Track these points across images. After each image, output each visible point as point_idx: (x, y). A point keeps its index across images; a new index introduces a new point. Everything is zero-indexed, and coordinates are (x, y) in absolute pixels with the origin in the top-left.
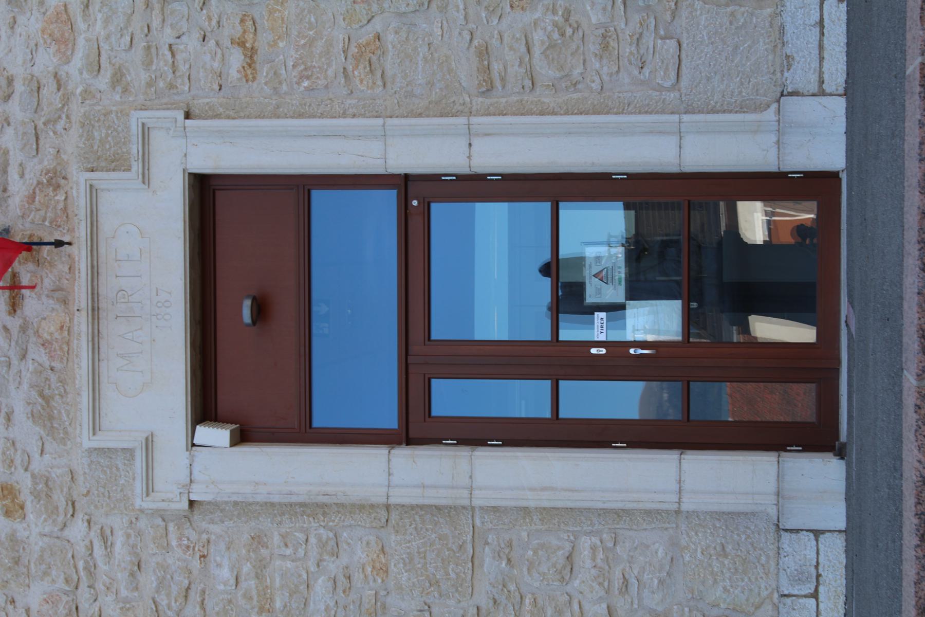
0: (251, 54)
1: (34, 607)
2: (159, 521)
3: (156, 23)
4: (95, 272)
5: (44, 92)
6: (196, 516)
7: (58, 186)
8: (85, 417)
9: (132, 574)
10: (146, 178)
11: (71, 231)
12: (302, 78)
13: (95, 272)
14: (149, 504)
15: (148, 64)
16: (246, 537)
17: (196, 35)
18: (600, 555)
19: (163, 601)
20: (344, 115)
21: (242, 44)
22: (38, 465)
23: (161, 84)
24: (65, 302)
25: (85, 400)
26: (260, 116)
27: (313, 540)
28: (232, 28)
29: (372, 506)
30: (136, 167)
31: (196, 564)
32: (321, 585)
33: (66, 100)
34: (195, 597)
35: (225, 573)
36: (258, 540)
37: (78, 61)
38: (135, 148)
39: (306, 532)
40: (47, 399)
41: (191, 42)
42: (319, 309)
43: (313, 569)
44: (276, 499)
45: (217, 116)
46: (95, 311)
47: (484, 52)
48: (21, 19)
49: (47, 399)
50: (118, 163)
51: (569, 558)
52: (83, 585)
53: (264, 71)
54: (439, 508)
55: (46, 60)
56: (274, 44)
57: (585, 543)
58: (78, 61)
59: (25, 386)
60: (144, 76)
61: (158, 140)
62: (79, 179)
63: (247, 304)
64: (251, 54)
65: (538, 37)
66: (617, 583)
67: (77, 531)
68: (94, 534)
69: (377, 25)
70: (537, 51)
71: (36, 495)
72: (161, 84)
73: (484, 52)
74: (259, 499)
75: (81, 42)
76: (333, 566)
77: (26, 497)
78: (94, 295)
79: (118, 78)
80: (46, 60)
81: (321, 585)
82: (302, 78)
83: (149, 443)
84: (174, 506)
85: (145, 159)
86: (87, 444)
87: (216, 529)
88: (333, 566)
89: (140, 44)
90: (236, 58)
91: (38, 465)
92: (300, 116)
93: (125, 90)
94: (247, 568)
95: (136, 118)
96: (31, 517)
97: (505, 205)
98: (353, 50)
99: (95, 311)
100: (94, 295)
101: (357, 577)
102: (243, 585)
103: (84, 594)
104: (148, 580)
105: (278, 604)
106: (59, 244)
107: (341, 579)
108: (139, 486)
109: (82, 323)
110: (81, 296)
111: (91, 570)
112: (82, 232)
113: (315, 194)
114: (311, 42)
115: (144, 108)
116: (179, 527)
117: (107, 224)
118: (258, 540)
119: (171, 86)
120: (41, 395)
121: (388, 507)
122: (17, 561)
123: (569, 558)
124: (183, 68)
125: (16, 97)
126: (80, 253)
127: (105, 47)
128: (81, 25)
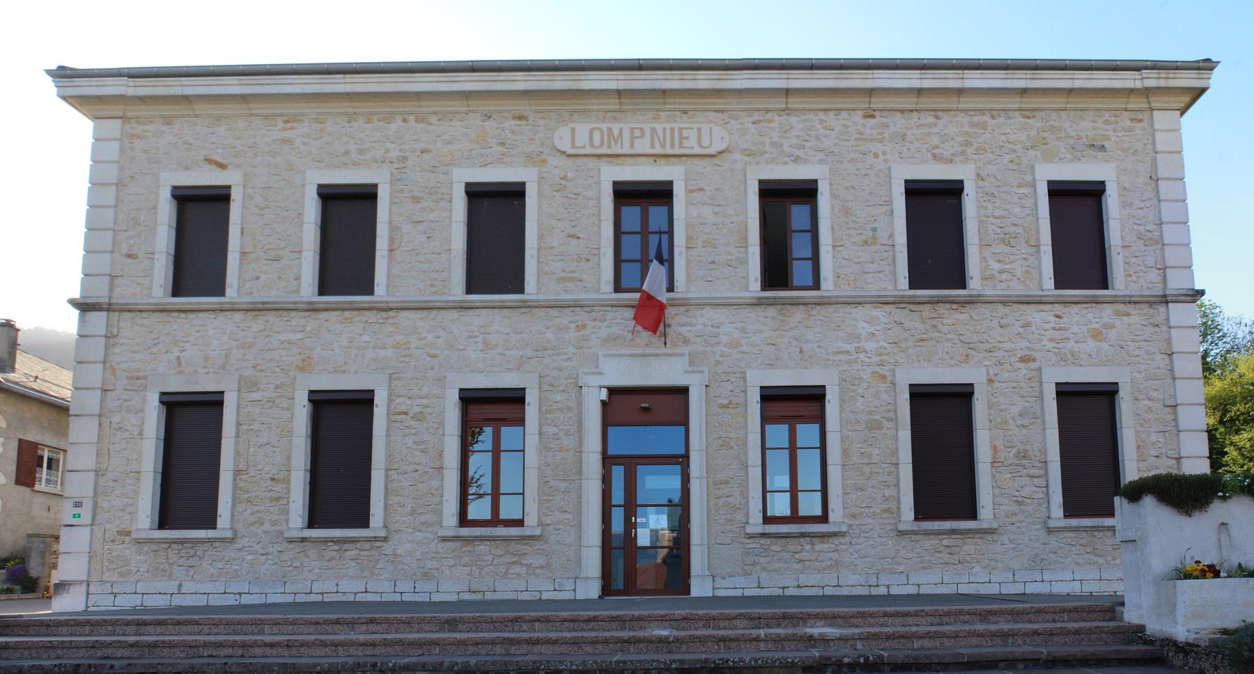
0: (726, 406)
1: (546, 335)
2: (575, 376)
3: (736, 375)
4: (656, 355)
5: (715, 339)
6: (577, 388)
7: (684, 343)
8: (609, 352)
9: (557, 368)
10: (687, 372)
11: (670, 347)
12: (719, 423)
13: (656, 355)
14: (580, 373)
15: (723, 373)
16: (570, 405)
17: (733, 389)
18: (567, 521)
19: (547, 378)
20: (707, 437)
21: (730, 404)
22: (593, 336)
23: (717, 377)
24: (647, 345)
25: (615, 352)
26: (706, 409)
27: (570, 427)
28: (735, 400)
29: (581, 447)
30: (690, 369)
31: (561, 388)
32: (555, 430)
33: (712, 345)
34: (550, 388)
35: (558, 398)
36: (569, 409)
37: (724, 349)
38: (696, 369)
39: (573, 425)
40: (615, 339)
41: (730, 387)
42: (648, 428)
43: (561, 427)
44: (583, 415)
45: (706, 395)
46: (644, 355)
47: (727, 482)
48: (738, 331)
49: (615, 339)
50: (691, 363)
51: (566, 511)
52: (553, 352)
53: (721, 411)
54: (581, 469)
55: (725, 339)
56: (730, 414)
57: (571, 516)
58: (724, 349)
59: (619, 332)
60: (719, 372)
61: (699, 376)
62: (686, 350)
63: (647, 405)
64: (726, 406)
65: (732, 499)
66: (558, 527)
67: (572, 349)
68: (571, 355)
69: (736, 448)
70: (727, 499)
71: (583, 336)
72: (717, 377)
73: (727, 482)
74: (583, 410)
75: (731, 350)
76: (561, 434)
77: (583, 332)
78: (649, 355)
79: (718, 363)
80: (725, 339)
81: (555, 430)
82: (719, 423)
83: (600, 373)
84: (580, 381)
85: (693, 372)
86: (600, 353)
87: (573, 395)
88: (561, 434)
89: (730, 370)
90: (725, 402)
91: (593, 336)
92: (707, 423)
93: (715, 365)
94: (560, 405)
95: (706, 369)
96: (576, 334)
97: (680, 487)
98: (728, 440)
99: (644, 355)
100: (649, 355)
101: (558, 442)
102: (554, 404)
103: (551, 352)
104: (555, 373)
105: (549, 416)
106: (665, 343)
107: (557, 437)
108: (586, 370)
109: (640, 351)
110: (648, 351)
111: (558, 354)
112: (669, 351)
113: (683, 427)
114: (730, 426)
115: (709, 371)
116: (573, 383)
117: (672, 359)
118: (569, 409)
119: (716, 381)
120: (616, 338)
121: (581, 452)
122: (561, 329)
123: (566, 511)
124: (722, 384)
125: (712, 329)
126: (663, 350)
127: (729, 358)
128: (736, 351)
